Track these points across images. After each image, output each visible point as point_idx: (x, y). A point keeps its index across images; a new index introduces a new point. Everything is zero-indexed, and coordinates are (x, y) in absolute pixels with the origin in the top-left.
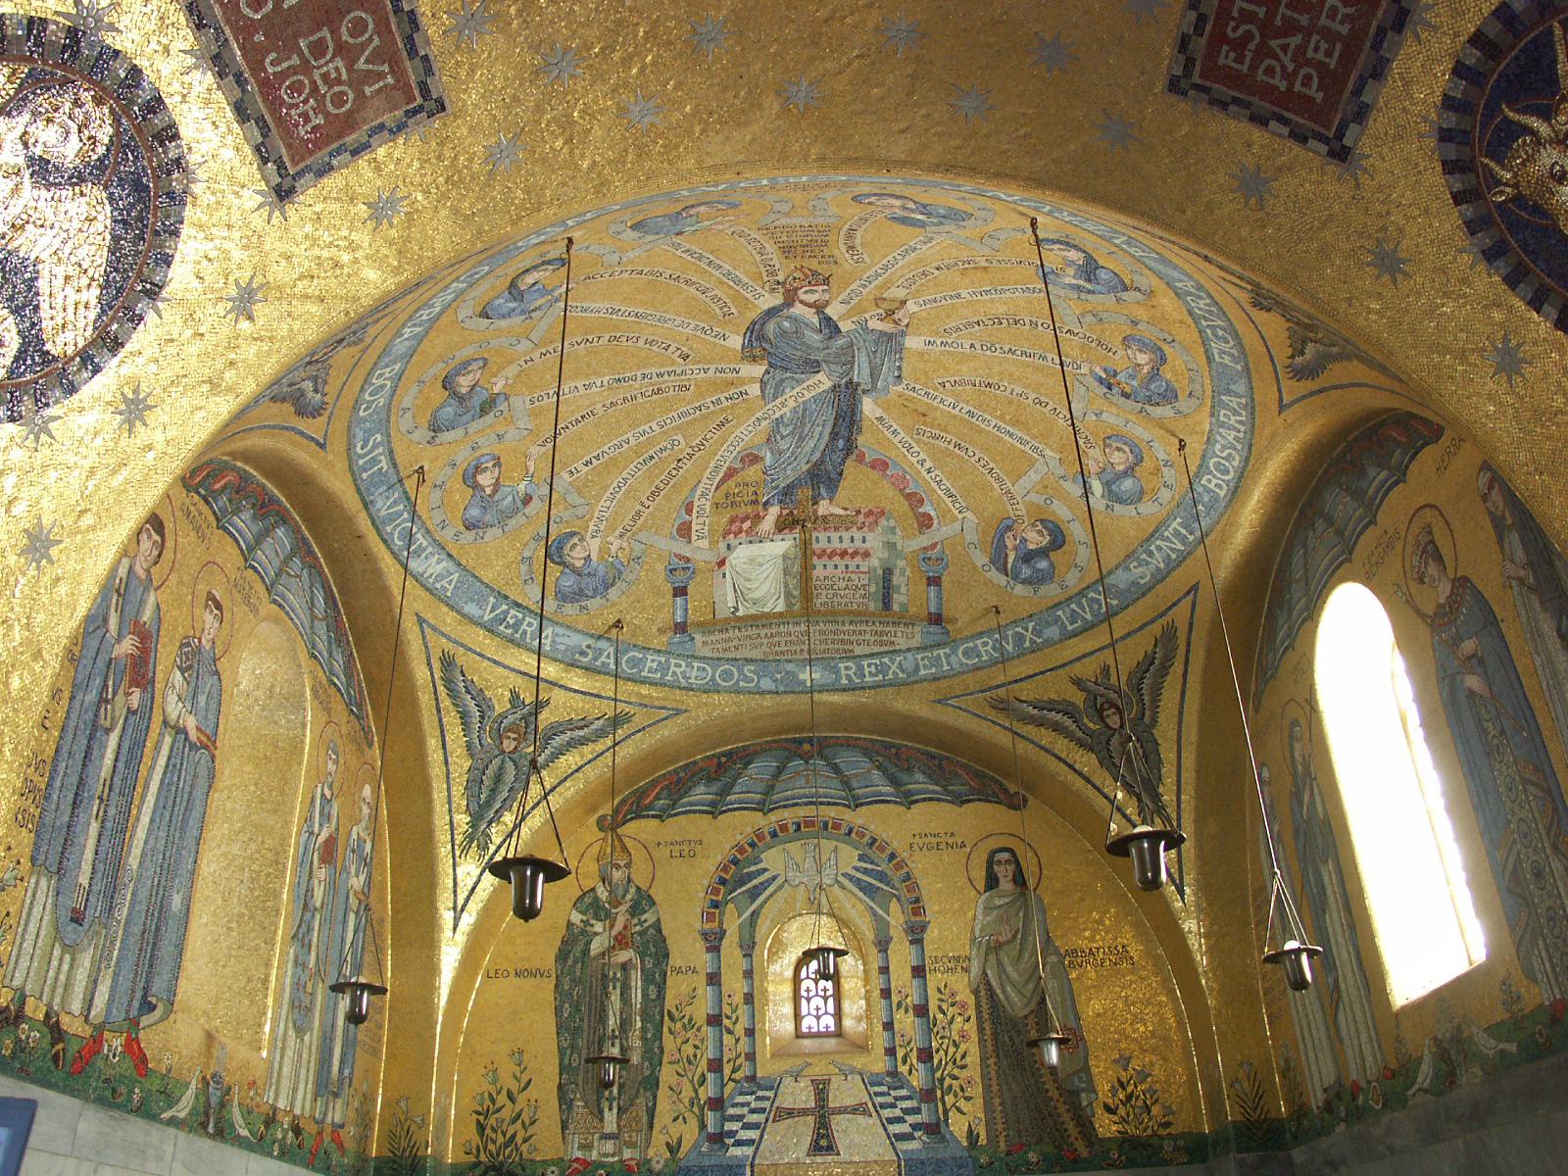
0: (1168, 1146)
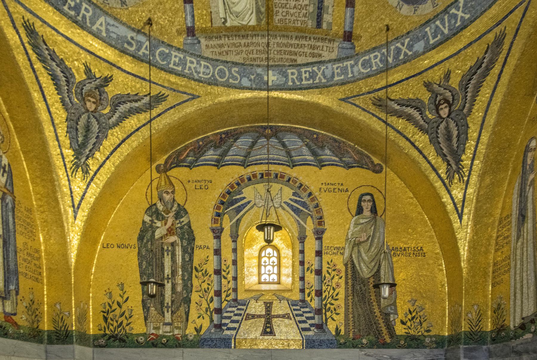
0: (427, 340)
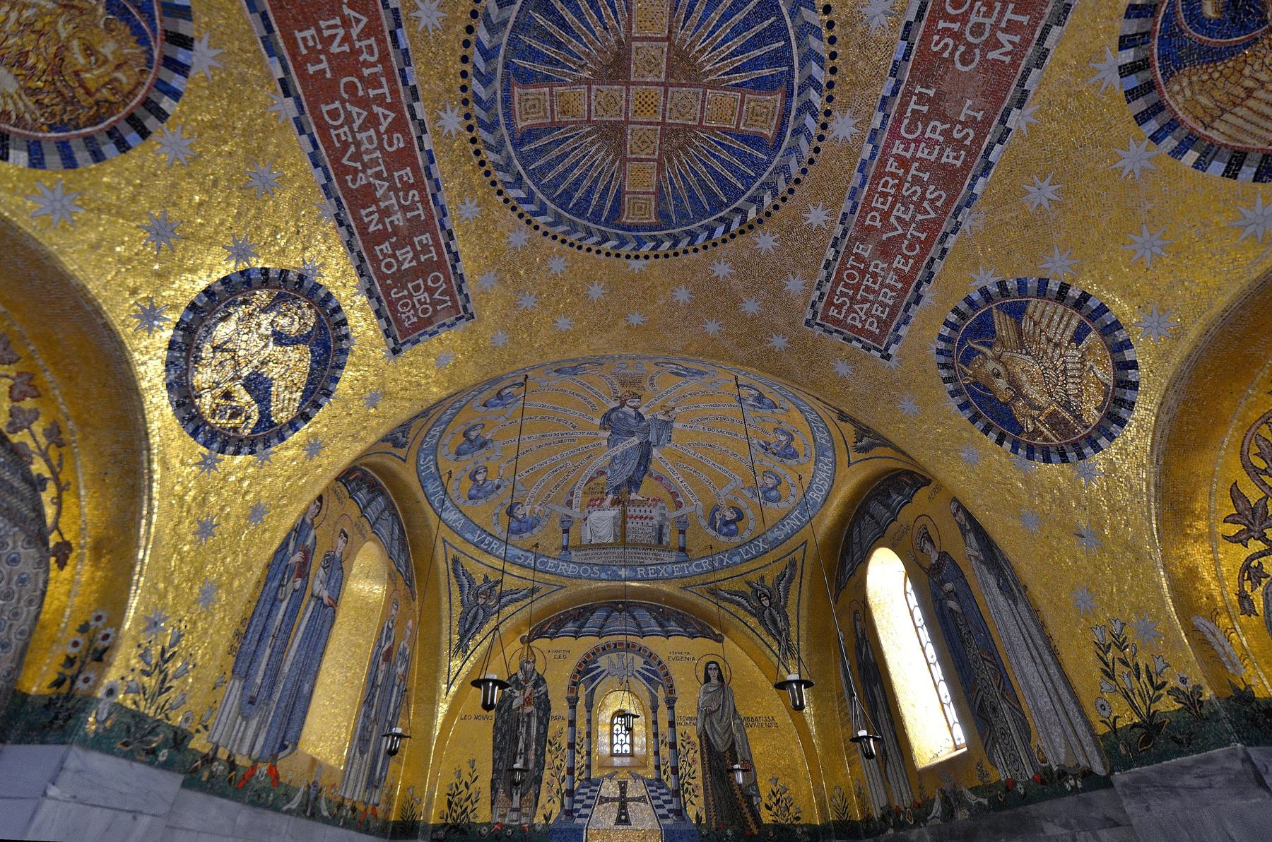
0: (799, 831)
